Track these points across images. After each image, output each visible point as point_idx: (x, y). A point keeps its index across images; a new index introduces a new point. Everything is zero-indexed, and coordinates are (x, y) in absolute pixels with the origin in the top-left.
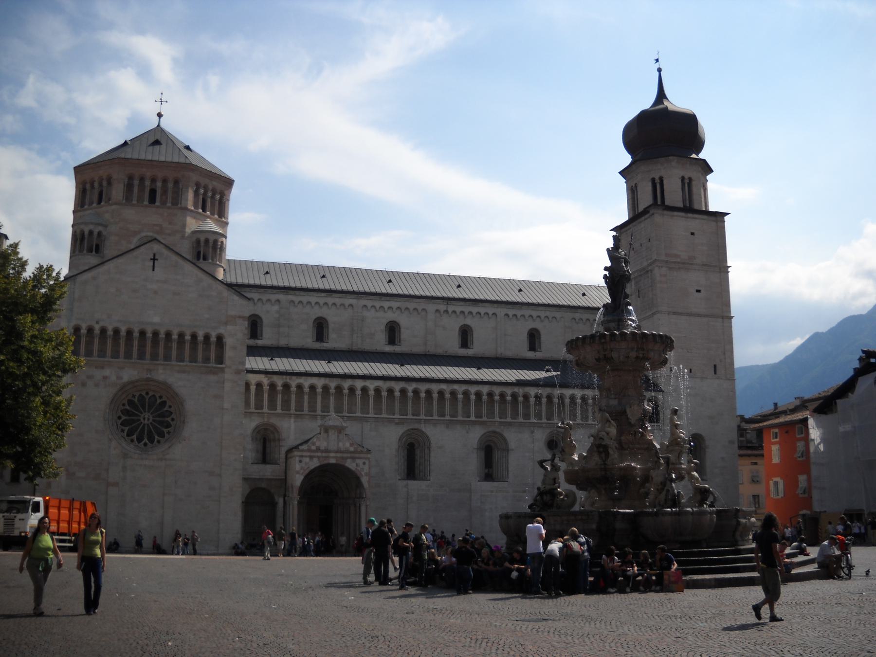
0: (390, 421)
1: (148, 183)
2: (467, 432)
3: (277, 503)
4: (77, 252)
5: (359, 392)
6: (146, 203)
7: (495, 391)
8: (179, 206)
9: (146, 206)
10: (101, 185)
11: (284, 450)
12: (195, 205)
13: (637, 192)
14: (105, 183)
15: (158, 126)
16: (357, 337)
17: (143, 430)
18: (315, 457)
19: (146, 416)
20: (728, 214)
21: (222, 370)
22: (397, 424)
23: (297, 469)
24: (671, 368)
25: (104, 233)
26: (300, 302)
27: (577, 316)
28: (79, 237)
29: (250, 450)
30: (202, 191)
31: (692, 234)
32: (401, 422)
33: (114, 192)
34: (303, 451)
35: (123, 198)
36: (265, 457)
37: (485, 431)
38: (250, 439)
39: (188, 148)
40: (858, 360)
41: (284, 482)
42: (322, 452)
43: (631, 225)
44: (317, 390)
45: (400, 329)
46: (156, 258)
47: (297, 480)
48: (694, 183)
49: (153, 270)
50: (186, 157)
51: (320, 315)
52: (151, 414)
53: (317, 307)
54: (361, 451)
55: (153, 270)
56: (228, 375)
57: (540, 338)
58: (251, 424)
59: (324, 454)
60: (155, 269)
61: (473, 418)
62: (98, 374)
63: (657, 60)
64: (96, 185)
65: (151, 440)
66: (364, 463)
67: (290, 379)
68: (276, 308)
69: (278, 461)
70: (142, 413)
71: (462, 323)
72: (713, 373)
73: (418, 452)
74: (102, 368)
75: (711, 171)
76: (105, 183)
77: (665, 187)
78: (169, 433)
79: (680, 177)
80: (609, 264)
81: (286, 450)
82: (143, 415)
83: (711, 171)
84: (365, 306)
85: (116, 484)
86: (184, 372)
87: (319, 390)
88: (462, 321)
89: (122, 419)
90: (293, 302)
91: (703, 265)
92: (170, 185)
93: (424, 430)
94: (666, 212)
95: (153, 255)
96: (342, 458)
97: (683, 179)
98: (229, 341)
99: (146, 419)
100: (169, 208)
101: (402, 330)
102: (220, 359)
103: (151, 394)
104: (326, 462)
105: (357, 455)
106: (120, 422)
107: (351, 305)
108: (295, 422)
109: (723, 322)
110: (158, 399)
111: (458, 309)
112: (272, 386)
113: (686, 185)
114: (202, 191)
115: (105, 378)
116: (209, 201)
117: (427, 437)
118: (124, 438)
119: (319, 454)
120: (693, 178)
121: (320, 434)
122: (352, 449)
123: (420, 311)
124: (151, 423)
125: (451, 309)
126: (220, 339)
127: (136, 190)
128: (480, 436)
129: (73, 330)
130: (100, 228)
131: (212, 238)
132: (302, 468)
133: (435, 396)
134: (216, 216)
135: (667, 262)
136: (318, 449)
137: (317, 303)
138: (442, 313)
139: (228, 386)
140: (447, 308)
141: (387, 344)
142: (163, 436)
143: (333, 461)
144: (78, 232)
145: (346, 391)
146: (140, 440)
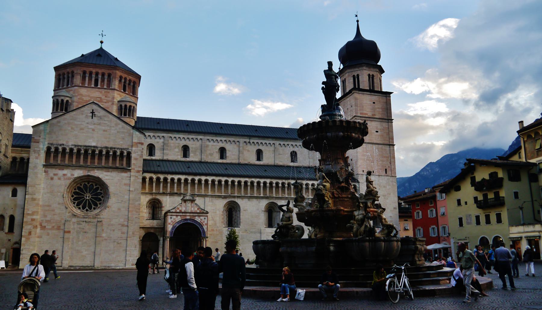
0: (219, 197)
1: (94, 76)
2: (259, 203)
3: (159, 240)
4: (55, 111)
5: (203, 182)
6: (93, 86)
7: (273, 182)
8: (111, 88)
9: (93, 88)
10: (68, 77)
11: (163, 213)
12: (119, 86)
13: (345, 82)
14: (70, 75)
15: (101, 48)
16: (204, 155)
17: (86, 202)
18: (179, 215)
19: (88, 195)
20: (392, 93)
21: (130, 171)
22: (223, 198)
23: (169, 222)
24: (363, 170)
25: (70, 101)
26: (175, 137)
28: (55, 103)
29: (145, 212)
30: (123, 81)
31: (374, 103)
32: (225, 197)
33: (75, 80)
34: (172, 212)
35: (80, 83)
36: (154, 217)
37: (268, 202)
38: (146, 207)
39: (116, 59)
40: (464, 164)
41: (163, 229)
42: (183, 213)
43: (342, 100)
44: (182, 181)
45: (226, 151)
46: (94, 112)
47: (169, 228)
48: (374, 77)
49: (92, 118)
50: (115, 63)
51: (185, 144)
52: (91, 194)
53: (183, 140)
54: (204, 213)
55: (92, 118)
56: (132, 174)
57: (297, 156)
58: (145, 200)
59: (184, 214)
60: (93, 118)
61: (262, 195)
62: (61, 173)
63: (356, 16)
64: (66, 76)
65: (90, 208)
66: (205, 219)
67: (167, 176)
68: (162, 140)
69: (160, 218)
70: (85, 194)
71: (258, 148)
73: (234, 213)
74: (63, 169)
75: (384, 72)
76: (70, 75)
77: (360, 79)
78: (100, 204)
80: (325, 80)
81: (164, 212)
82: (85, 195)
83: (384, 72)
84: (208, 140)
85: (69, 232)
86: (109, 171)
87: (183, 181)
88: (257, 147)
89: (74, 197)
91: (379, 119)
92: (106, 77)
93: (237, 201)
94: (360, 92)
95: (92, 110)
96: (193, 216)
97: (369, 75)
98: (133, 155)
99: (88, 197)
100: (105, 89)
101: (227, 152)
102: (129, 164)
103: (90, 183)
104: (184, 218)
105: (201, 215)
106: (72, 198)
107: (201, 139)
108: (169, 198)
109: (390, 147)
110: (94, 186)
111: (255, 141)
113: (371, 79)
114: (123, 81)
115: (64, 175)
116: (127, 85)
117: (239, 205)
118: (75, 207)
119: (181, 214)
120: (374, 75)
121: (182, 203)
122: (198, 211)
123: (236, 142)
124: (90, 199)
125: (252, 141)
126: (129, 154)
127: (87, 79)
128: (266, 204)
129: (46, 150)
130: (68, 99)
131: (128, 104)
132: (172, 221)
133: (243, 184)
134: (131, 94)
135: (361, 117)
136: (181, 212)
137: (184, 138)
138: (247, 143)
139: (132, 178)
140: (250, 140)
141: (219, 158)
142: (97, 206)
143: (188, 217)
144: (55, 100)
145: (196, 182)
146: (84, 208)
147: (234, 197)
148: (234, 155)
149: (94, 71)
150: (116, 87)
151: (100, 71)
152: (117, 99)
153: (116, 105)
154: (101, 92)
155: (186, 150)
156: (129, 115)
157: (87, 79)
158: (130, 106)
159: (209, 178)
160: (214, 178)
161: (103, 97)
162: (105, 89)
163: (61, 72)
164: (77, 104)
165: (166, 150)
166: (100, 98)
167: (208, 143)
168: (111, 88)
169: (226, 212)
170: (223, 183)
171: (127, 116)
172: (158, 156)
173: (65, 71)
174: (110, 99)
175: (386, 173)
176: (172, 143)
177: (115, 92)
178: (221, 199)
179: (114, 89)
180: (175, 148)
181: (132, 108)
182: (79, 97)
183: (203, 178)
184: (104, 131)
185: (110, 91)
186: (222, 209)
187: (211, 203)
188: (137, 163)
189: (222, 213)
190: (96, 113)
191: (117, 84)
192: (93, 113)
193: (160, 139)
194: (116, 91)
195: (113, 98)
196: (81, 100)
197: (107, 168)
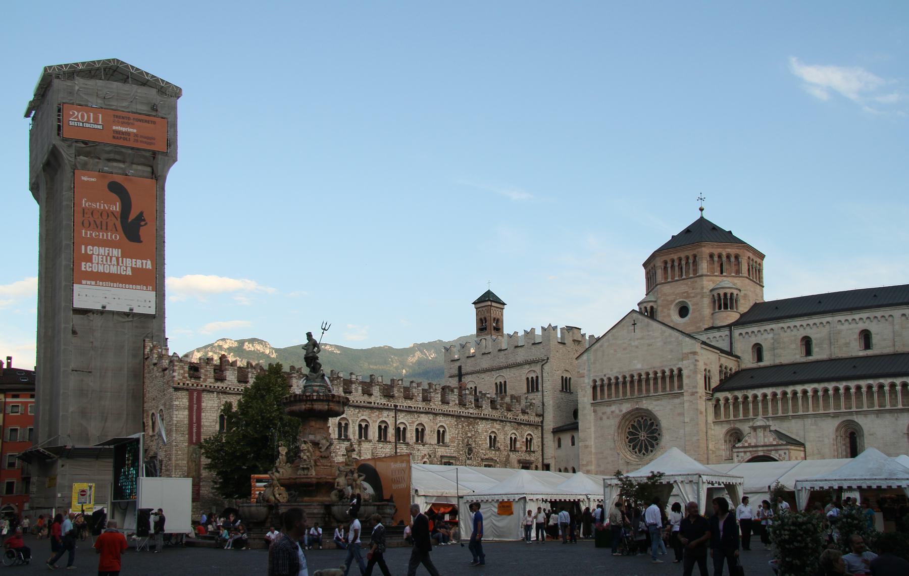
0: (827, 415)
1: (676, 264)
8: (698, 274)
9: (677, 281)
22: (833, 417)
25: (655, 307)
32: (836, 416)
68: (771, 335)
73: (858, 440)
76: (654, 272)
90: (783, 328)
92: (691, 261)
93: (856, 420)
100: (691, 278)
127: (669, 269)
130: (651, 304)
131: (722, 292)
147: (851, 413)
149: (675, 257)
150: (705, 272)
151: (683, 255)
152: (709, 287)
153: (708, 297)
155: (807, 342)
157: (669, 269)
158: (725, 294)
159: (808, 387)
160: (815, 386)
162: (691, 278)
163: (648, 269)
164: (661, 308)
165: (777, 349)
168: (698, 274)
169: (844, 439)
170: (831, 392)
171: (722, 309)
172: (767, 361)
173: (650, 267)
174: (699, 290)
176: (786, 336)
177: (704, 280)
178: (829, 418)
179: (702, 276)
180: (791, 344)
181: (729, 296)
182: (662, 299)
183: (799, 388)
185: (698, 279)
186: (833, 436)
187: (814, 427)
188: (694, 382)
189: (832, 442)
191: (706, 267)
193: (769, 334)
194: (704, 277)
195: (702, 288)
196: (665, 302)
197: (658, 398)
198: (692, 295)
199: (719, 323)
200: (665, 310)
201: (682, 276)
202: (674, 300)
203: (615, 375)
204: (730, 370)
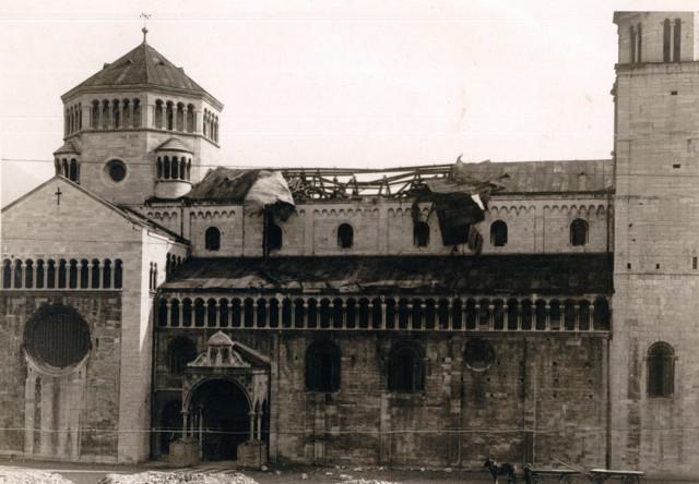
25: (78, 160)
27: (551, 203)
68: (232, 219)
72: (691, 266)
79: (663, 20)
100: (131, 130)
102: (119, 284)
112: (187, 302)
126: (119, 262)
130: (74, 156)
148: (368, 238)
154: (124, 137)
156: (182, 178)
161: (129, 147)
166: (123, 148)
167: (317, 217)
171: (170, 179)
174: (139, 149)
175: (695, 266)
184: (79, 224)
185: (141, 134)
190: (63, 195)
192: (59, 194)
198: (131, 153)
199: (162, 194)
200: (93, 168)
201: (117, 125)
202: (106, 157)
203: (27, 258)
204: (179, 258)
